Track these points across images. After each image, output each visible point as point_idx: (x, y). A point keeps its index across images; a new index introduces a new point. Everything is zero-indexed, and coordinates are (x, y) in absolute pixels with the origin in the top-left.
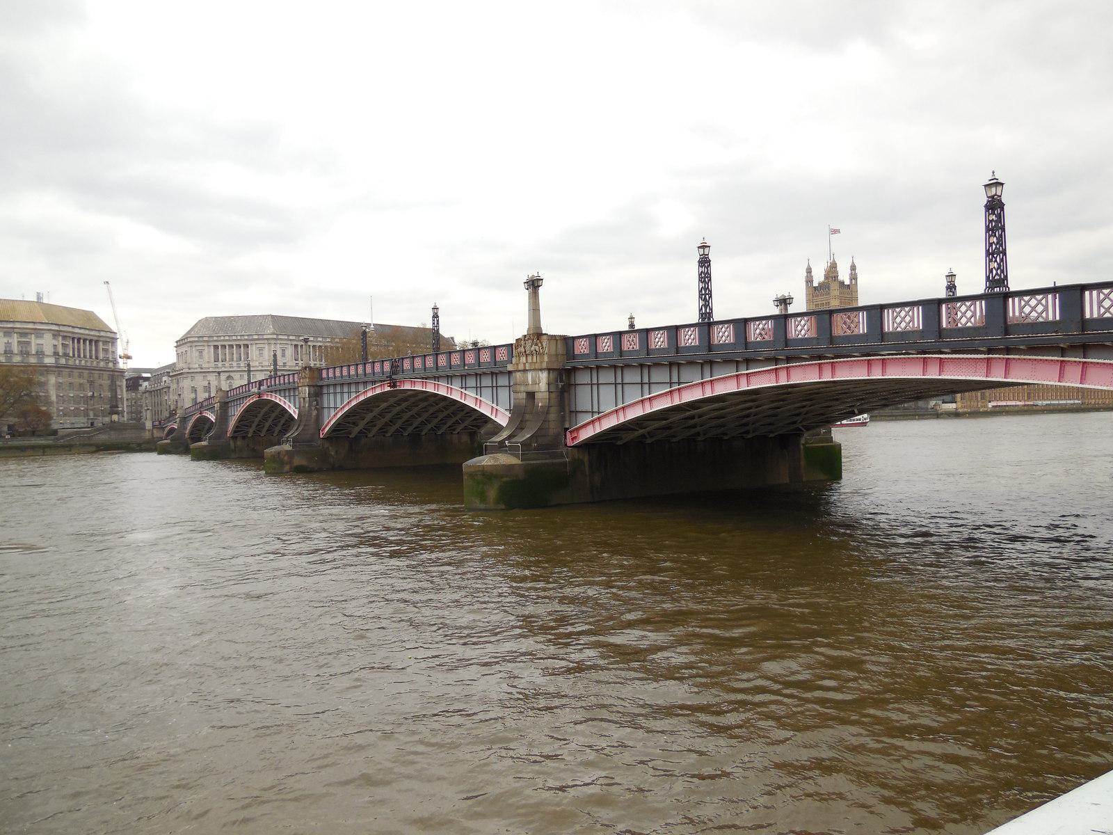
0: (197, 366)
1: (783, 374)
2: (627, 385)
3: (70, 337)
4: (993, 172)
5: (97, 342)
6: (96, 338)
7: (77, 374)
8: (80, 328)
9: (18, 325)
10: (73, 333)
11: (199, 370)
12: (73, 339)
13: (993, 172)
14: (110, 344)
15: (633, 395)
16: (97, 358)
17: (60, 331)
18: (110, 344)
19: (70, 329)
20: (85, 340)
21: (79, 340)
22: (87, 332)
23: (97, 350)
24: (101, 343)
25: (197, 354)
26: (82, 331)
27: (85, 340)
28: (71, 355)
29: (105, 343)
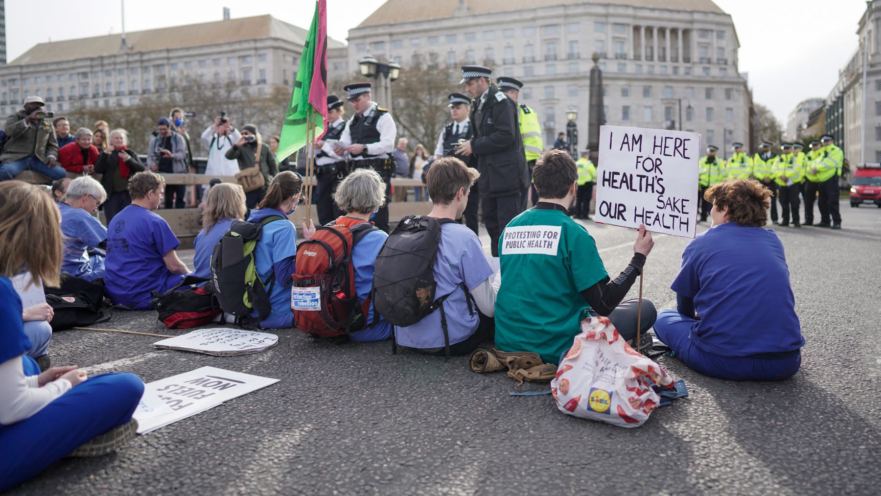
3: (628, 25)
5: (686, 32)
6: (688, 26)
7: (641, 90)
8: (653, 10)
10: (635, 17)
12: (637, 29)
14: (715, 34)
17: (606, 16)
18: (715, 34)
19: (630, 12)
22: (667, 15)
23: (687, 47)
24: (695, 37)
28: (631, 55)
29: (704, 32)
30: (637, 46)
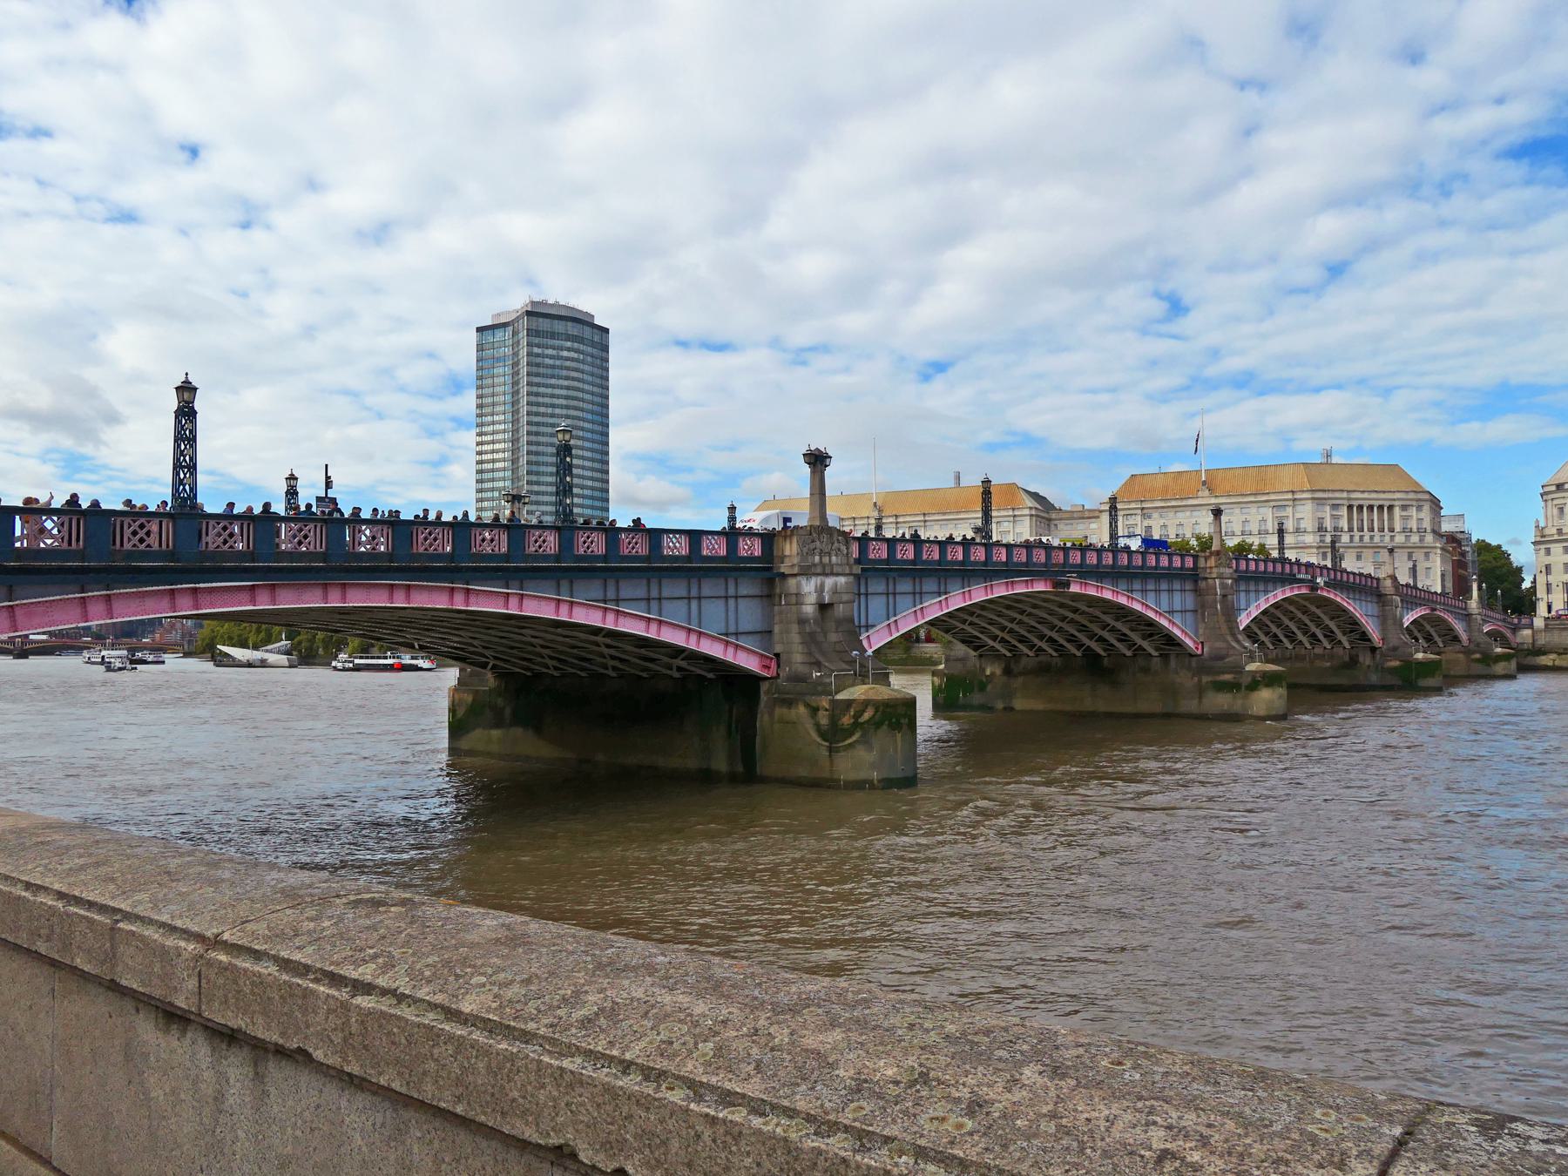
0: (1554, 531)
1: (513, 601)
2: (708, 600)
4: (187, 374)
5: (1391, 508)
9: (1273, 497)
10: (1349, 499)
11: (1556, 537)
13: (187, 374)
15: (1262, 600)
16: (1392, 530)
20: (1371, 508)
21: (1360, 508)
22: (1374, 495)
23: (1391, 518)
24: (1397, 511)
25: (1555, 511)
26: (1366, 495)
27: (1371, 508)
29: (1404, 508)
30: (1350, 520)
